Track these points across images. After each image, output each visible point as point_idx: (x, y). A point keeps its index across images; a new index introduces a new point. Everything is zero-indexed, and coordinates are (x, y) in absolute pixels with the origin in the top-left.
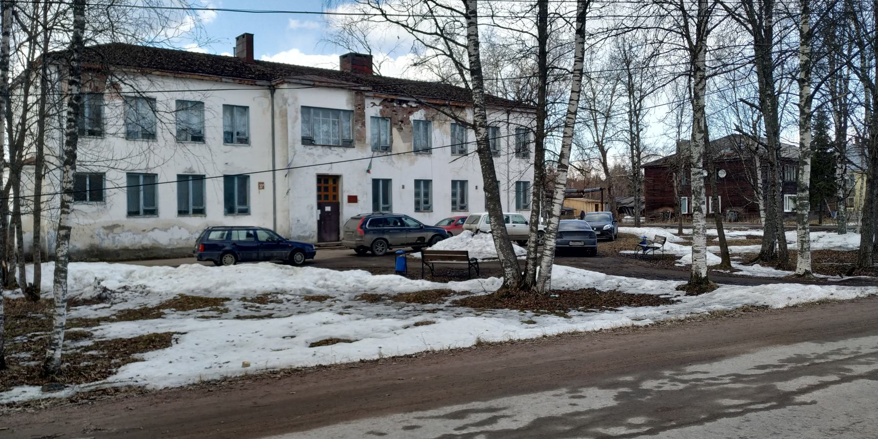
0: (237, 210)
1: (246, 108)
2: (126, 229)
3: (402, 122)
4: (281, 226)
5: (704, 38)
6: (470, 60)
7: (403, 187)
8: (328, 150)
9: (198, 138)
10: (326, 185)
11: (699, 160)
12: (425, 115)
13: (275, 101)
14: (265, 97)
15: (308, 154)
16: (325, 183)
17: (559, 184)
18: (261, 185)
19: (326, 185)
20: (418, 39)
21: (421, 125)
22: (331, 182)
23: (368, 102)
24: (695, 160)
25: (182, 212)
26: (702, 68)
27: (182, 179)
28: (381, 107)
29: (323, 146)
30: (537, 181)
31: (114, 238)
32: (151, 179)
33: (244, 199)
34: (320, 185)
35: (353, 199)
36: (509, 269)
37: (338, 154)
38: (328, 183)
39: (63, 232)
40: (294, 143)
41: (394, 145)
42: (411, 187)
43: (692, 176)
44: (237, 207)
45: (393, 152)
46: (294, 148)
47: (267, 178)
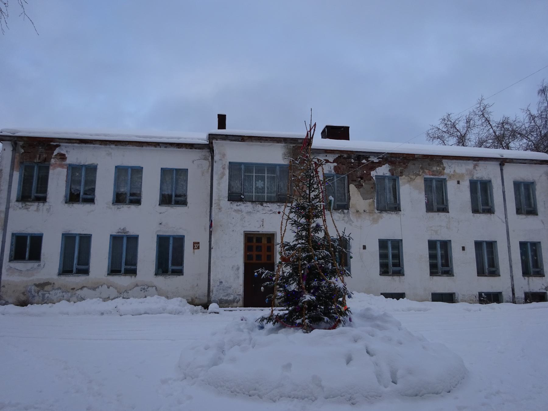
0: (170, 270)
2: (56, 286)
3: (362, 178)
7: (364, 247)
8: (259, 207)
12: (390, 171)
14: (206, 159)
15: (235, 211)
18: (196, 246)
21: (387, 181)
25: (114, 271)
27: (116, 239)
28: (335, 164)
31: (44, 295)
32: (86, 239)
33: (179, 260)
37: (271, 210)
40: (219, 200)
41: (352, 202)
42: (374, 249)
44: (171, 267)
45: (352, 210)
46: (219, 205)
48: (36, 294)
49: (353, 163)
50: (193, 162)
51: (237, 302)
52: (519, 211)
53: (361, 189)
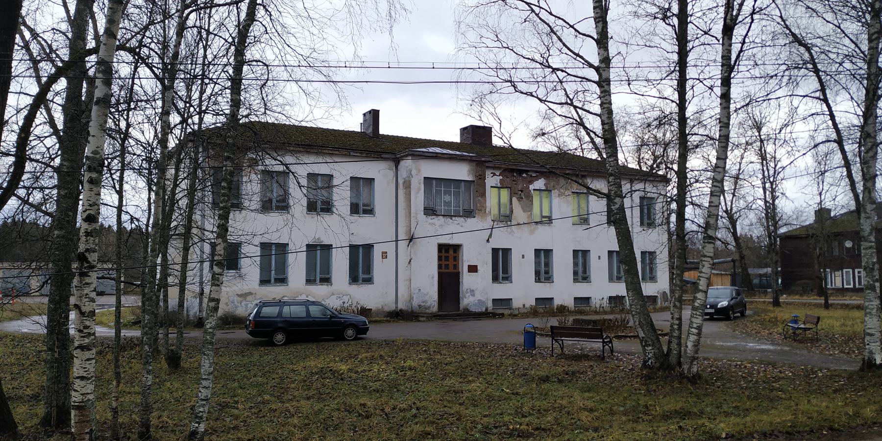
1: (371, 181)
3: (522, 191)
4: (403, 295)
5: (875, 102)
6: (603, 128)
9: (327, 208)
10: (447, 255)
11: (870, 234)
12: (545, 185)
13: (399, 172)
16: (445, 253)
17: (705, 256)
18: (384, 255)
19: (447, 255)
20: (550, 109)
22: (451, 252)
23: (488, 173)
24: (866, 234)
25: (309, 281)
26: (872, 135)
28: (501, 177)
29: (444, 216)
30: (680, 253)
31: (246, 305)
32: (282, 248)
33: (368, 269)
34: (441, 254)
35: (473, 269)
36: (650, 348)
38: (448, 253)
39: (212, 304)
40: (416, 214)
43: (863, 251)
44: (361, 276)
46: (416, 218)
47: (390, 248)
48: (239, 305)
49: (515, 177)
50: (379, 171)
51: (433, 307)
52: (642, 224)
53: (522, 202)
